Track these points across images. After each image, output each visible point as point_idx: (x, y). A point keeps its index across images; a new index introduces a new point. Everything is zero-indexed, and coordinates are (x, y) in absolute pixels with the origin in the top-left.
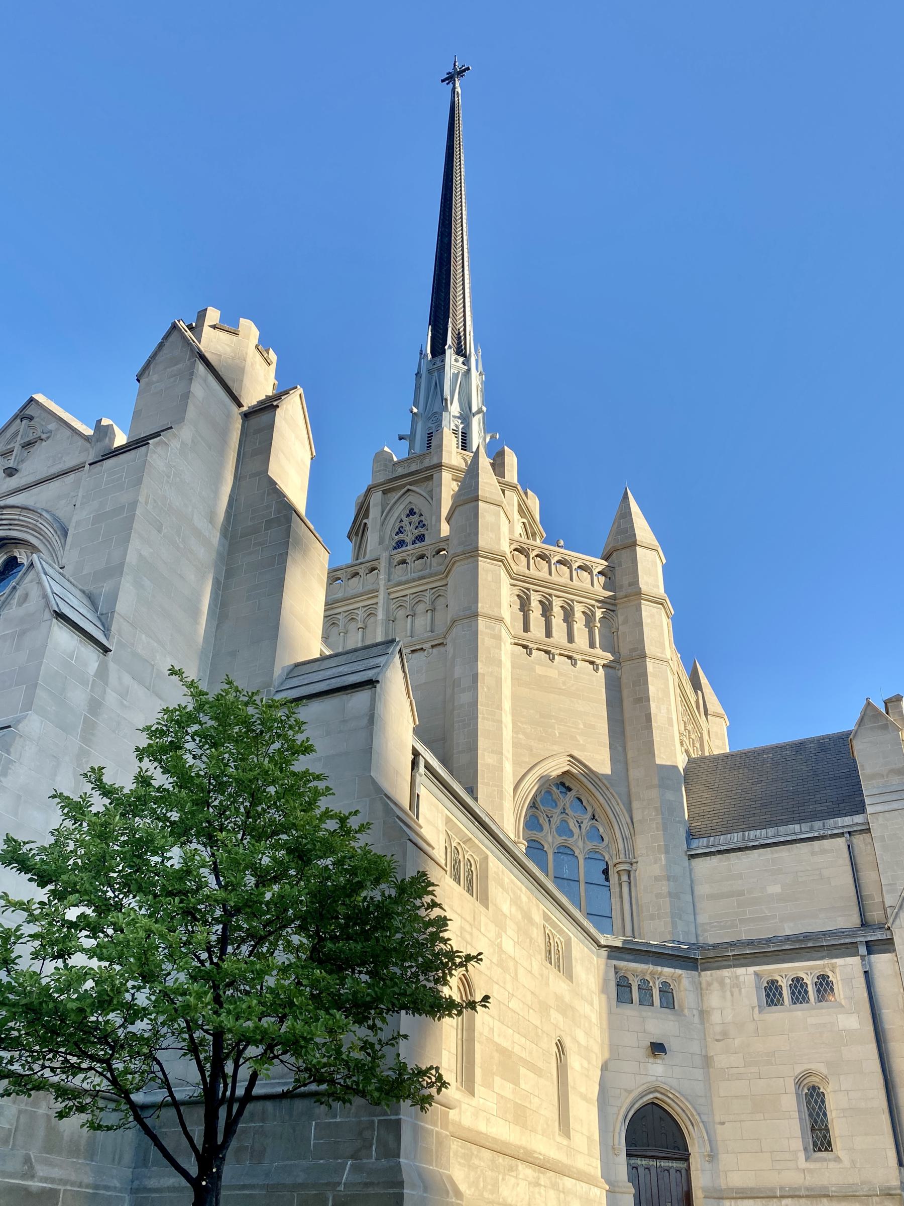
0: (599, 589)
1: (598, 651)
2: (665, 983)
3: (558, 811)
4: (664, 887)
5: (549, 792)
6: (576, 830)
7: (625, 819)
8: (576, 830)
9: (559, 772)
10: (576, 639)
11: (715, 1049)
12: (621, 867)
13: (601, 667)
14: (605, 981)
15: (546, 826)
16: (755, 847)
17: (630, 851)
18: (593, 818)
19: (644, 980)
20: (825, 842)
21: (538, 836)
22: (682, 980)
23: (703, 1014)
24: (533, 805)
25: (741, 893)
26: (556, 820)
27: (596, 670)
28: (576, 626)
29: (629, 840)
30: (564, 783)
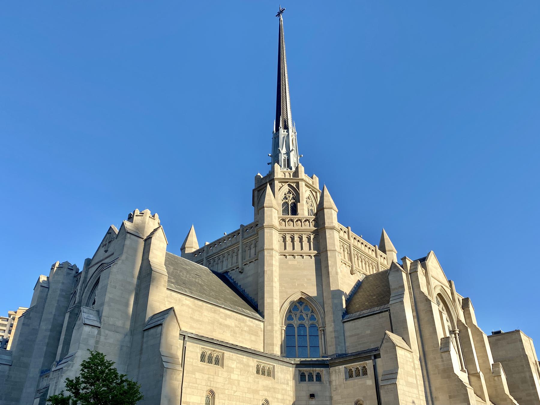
0: (313, 228)
1: (312, 251)
2: (318, 373)
3: (299, 312)
4: (333, 335)
5: (296, 306)
6: (306, 318)
7: (322, 311)
8: (306, 318)
9: (298, 298)
10: (304, 248)
11: (334, 394)
12: (321, 329)
13: (313, 257)
14: (295, 375)
15: (294, 318)
16: (362, 317)
17: (324, 323)
18: (312, 312)
19: (311, 373)
20: (383, 313)
21: (291, 322)
22: (323, 371)
23: (330, 382)
24: (289, 311)
25: (358, 334)
26: (298, 315)
27: (311, 258)
28: (303, 243)
29: (323, 318)
30: (301, 301)
